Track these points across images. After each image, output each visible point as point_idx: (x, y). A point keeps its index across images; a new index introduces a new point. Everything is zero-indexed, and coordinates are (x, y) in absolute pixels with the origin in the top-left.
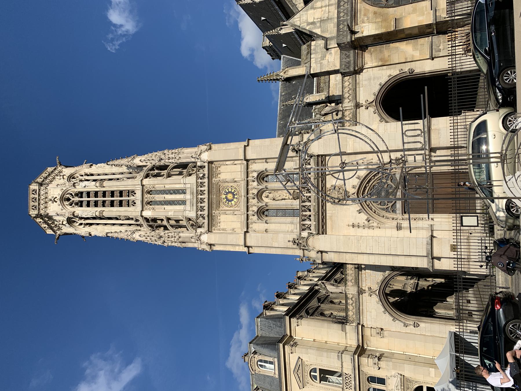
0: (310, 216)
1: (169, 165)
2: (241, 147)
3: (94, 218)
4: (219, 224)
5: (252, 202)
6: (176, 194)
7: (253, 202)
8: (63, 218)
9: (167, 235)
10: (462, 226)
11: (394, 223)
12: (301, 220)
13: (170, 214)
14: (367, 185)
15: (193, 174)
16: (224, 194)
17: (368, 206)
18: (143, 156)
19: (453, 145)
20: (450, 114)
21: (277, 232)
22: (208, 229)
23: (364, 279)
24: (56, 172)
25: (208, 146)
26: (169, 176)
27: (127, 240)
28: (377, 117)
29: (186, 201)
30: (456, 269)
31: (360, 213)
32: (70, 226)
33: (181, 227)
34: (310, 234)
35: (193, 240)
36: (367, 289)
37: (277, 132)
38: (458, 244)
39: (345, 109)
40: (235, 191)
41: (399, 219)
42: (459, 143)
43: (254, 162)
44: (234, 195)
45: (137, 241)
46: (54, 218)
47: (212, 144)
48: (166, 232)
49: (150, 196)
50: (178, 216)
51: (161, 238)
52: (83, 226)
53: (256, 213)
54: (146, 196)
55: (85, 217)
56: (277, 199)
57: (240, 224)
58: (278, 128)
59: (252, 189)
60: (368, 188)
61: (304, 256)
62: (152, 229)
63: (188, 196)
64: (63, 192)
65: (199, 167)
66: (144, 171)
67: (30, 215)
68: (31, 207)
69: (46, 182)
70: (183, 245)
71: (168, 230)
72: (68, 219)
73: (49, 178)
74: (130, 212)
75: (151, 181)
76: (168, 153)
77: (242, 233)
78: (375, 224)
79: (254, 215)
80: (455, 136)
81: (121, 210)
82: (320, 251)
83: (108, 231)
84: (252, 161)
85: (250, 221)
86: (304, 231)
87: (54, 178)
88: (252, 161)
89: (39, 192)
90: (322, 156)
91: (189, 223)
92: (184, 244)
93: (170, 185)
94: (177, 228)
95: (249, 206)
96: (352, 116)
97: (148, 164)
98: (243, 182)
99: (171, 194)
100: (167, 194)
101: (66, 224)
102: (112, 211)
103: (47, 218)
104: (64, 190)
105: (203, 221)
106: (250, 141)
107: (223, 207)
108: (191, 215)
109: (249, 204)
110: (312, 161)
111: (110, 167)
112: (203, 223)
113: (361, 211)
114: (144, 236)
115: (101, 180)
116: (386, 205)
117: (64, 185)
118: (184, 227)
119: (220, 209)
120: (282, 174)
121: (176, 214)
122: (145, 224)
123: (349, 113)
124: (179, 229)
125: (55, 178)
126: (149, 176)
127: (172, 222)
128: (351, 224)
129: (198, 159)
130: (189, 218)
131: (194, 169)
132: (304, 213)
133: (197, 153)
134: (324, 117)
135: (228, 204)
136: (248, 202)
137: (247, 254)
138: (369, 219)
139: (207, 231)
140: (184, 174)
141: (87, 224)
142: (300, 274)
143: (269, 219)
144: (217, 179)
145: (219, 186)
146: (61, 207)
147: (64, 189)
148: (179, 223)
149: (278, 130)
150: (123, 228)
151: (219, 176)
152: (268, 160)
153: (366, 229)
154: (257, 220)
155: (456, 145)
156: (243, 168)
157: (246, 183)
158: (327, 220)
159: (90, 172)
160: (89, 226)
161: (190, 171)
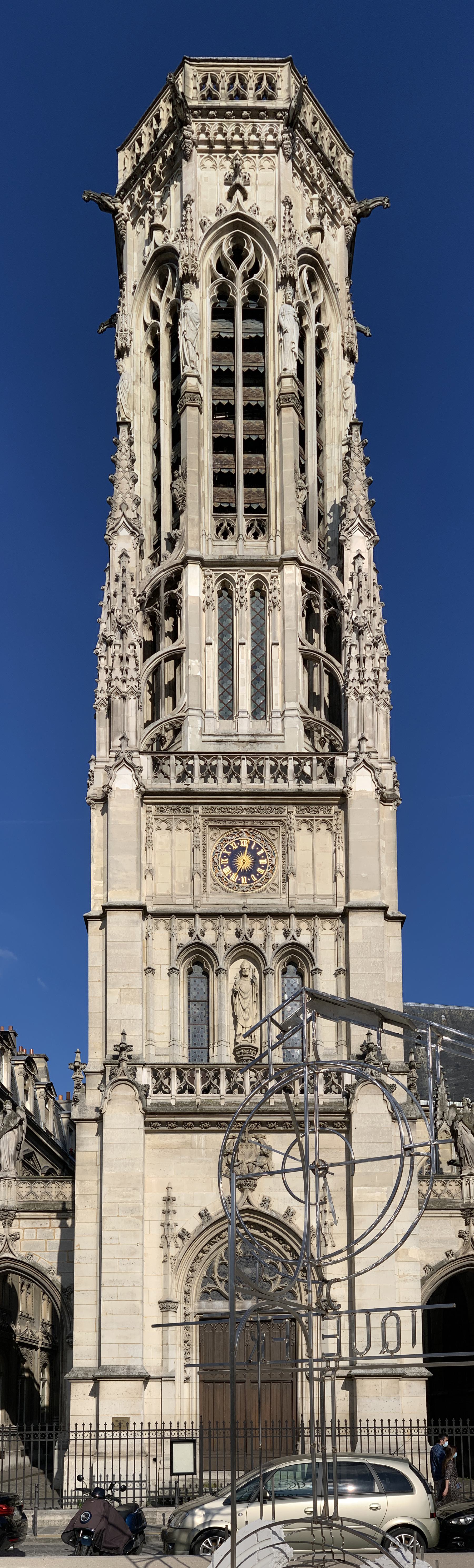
0: (192, 1091)
1: (340, 661)
2: (383, 897)
3: (176, 368)
4: (164, 826)
5: (228, 929)
6: (254, 684)
7: (229, 932)
8: (173, 230)
9: (129, 652)
10: (172, 1442)
11: (176, 1295)
12: (180, 1067)
13: (192, 665)
14: (270, 1234)
15: (310, 743)
16: (251, 842)
17: (218, 1235)
18: (373, 565)
19: (359, 1426)
20: (432, 1420)
21: (146, 1000)
22: (151, 790)
23: (37, 1224)
24: (335, 197)
25: (390, 793)
26: (309, 660)
27: (110, 503)
28: (436, 1258)
29: (231, 717)
30: (72, 1428)
31: (201, 1215)
32: (148, 260)
33: (155, 702)
34: (144, 1091)
35: (117, 742)
36: (13, 1230)
37: (417, 1005)
38: (130, 1433)
39: (464, 1181)
40: (258, 878)
41: (187, 1306)
42: (365, 1439)
43: (338, 935)
44: (248, 873)
45: (108, 545)
46: (172, 187)
47: (398, 805)
48: (139, 651)
49: (249, 590)
50: (188, 692)
51: (118, 633)
52: (150, 321)
53: (197, 941)
54: (248, 578)
55: (180, 333)
56: (236, 1001)
57: (165, 892)
58: (429, 1008)
59: (264, 929)
60: (263, 1235)
61: (87, 1074)
62: (146, 599)
63: (245, 725)
64: (264, 231)
65: (333, 761)
66: (325, 570)
67: (182, 65)
68: (210, 69)
69: (302, 149)
70: (103, 708)
71: (146, 657)
72: (170, 255)
73: (313, 164)
74: (197, 517)
75: (292, 595)
76: (377, 657)
77: (140, 898)
78: (173, 1251)
79: (191, 934)
80: (380, 1429)
81: (202, 480)
82: (102, 1115)
83: (135, 426)
84: (344, 931)
85: (176, 921)
86: (151, 1074)
87: (313, 187)
88: (342, 930)
89: (263, 109)
90: (348, 1124)
91: (167, 731)
92: (105, 713)
93: (279, 665)
94: (151, 686)
95: (216, 921)
96: (445, 1200)
97: (348, 584)
98: (284, 902)
99: (254, 667)
100: (254, 653)
101: (152, 244)
102: (200, 446)
103: (173, 152)
104: (272, 234)
105: (173, 776)
106: (399, 924)
107: (213, 840)
108: (190, 737)
109: (224, 921)
110: (335, 1098)
111: (344, 437)
112: (167, 777)
113: (206, 1218)
114: (124, 571)
115: (302, 400)
116: (221, 1278)
117: (287, 235)
118: (156, 714)
119: (208, 830)
120: (302, 1011)
121: (193, 686)
122: (160, 573)
123: (453, 1192)
124: (150, 697)
125: (314, 192)
126: (311, 589)
127: (168, 672)
128: (173, 1195)
129: (356, 759)
130: (180, 730)
131: (327, 744)
132: (198, 1076)
133: (373, 755)
134: (448, 1130)
135: (222, 857)
136: (228, 915)
137: (85, 914)
138: (185, 1237)
139: (143, 789)
140: (313, 711)
141: (156, 340)
142: (40, 1064)
143: (182, 980)
144: (294, 821)
145: (273, 828)
146: (214, 220)
147: (275, 235)
148: (166, 697)
149: (423, 1008)
150: (145, 489)
151: (304, 827)
152: (342, 976)
153: (161, 1231)
154: (180, 942)
155: (359, 1431)
156: (325, 902)
157: (281, 910)
158: (181, 1135)
159: (330, 350)
160: (149, 347)
161: (319, 732)
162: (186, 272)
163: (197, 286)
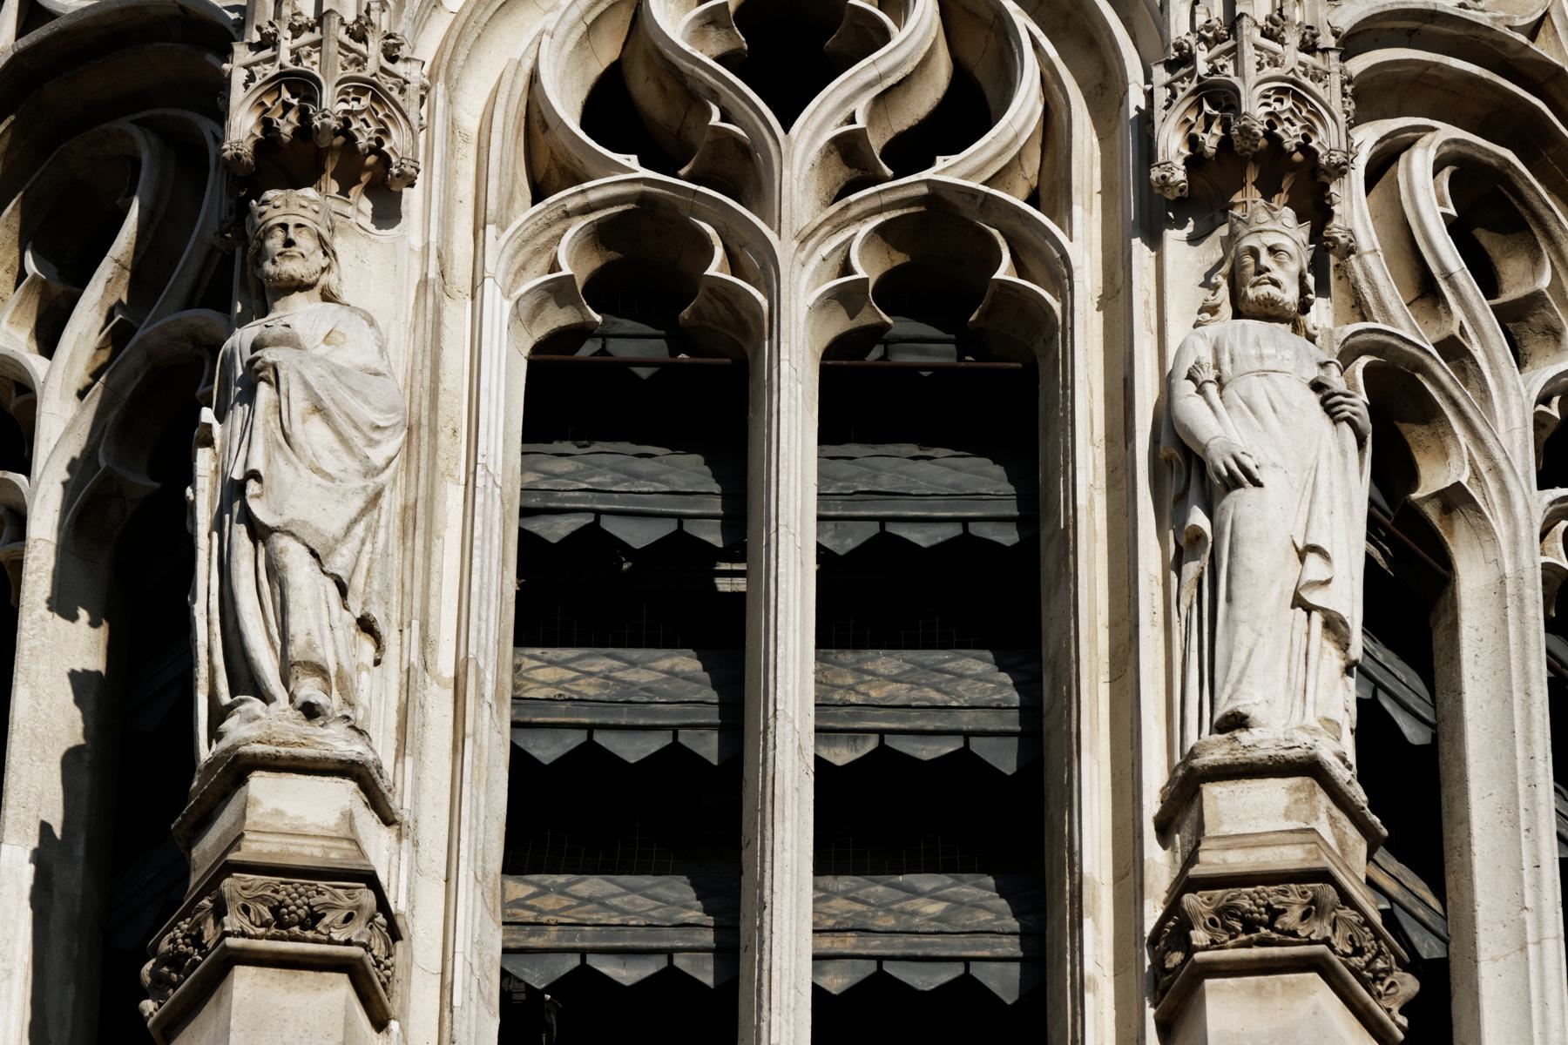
162: (287, 127)
163: (387, 213)
